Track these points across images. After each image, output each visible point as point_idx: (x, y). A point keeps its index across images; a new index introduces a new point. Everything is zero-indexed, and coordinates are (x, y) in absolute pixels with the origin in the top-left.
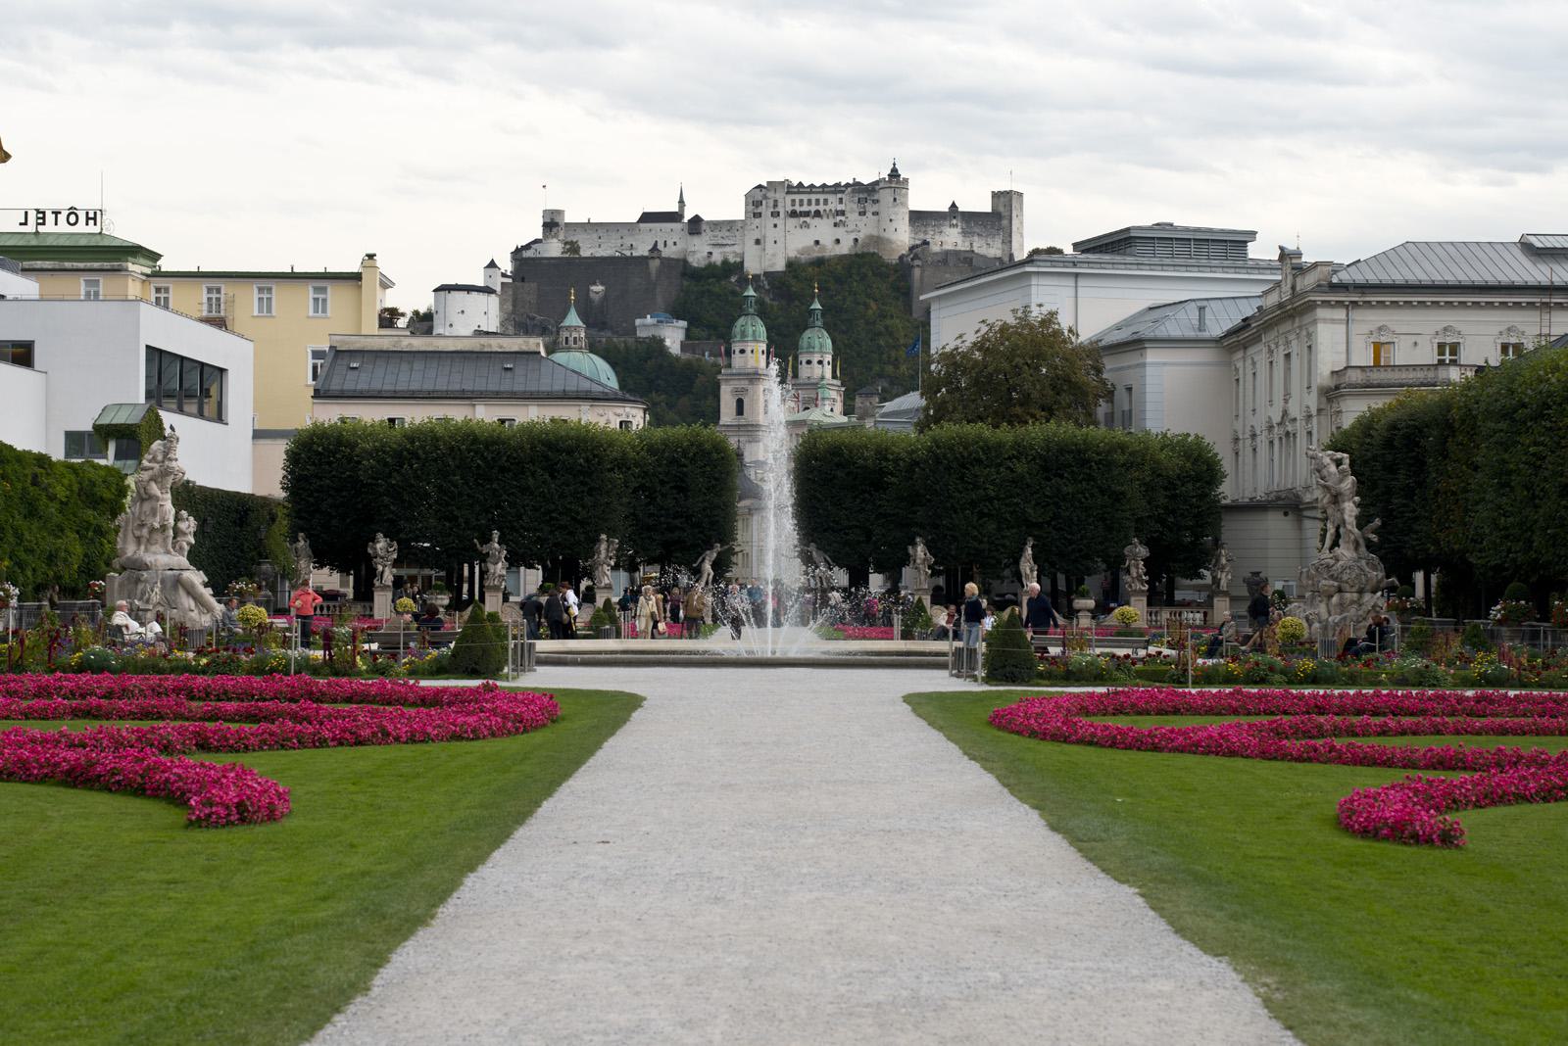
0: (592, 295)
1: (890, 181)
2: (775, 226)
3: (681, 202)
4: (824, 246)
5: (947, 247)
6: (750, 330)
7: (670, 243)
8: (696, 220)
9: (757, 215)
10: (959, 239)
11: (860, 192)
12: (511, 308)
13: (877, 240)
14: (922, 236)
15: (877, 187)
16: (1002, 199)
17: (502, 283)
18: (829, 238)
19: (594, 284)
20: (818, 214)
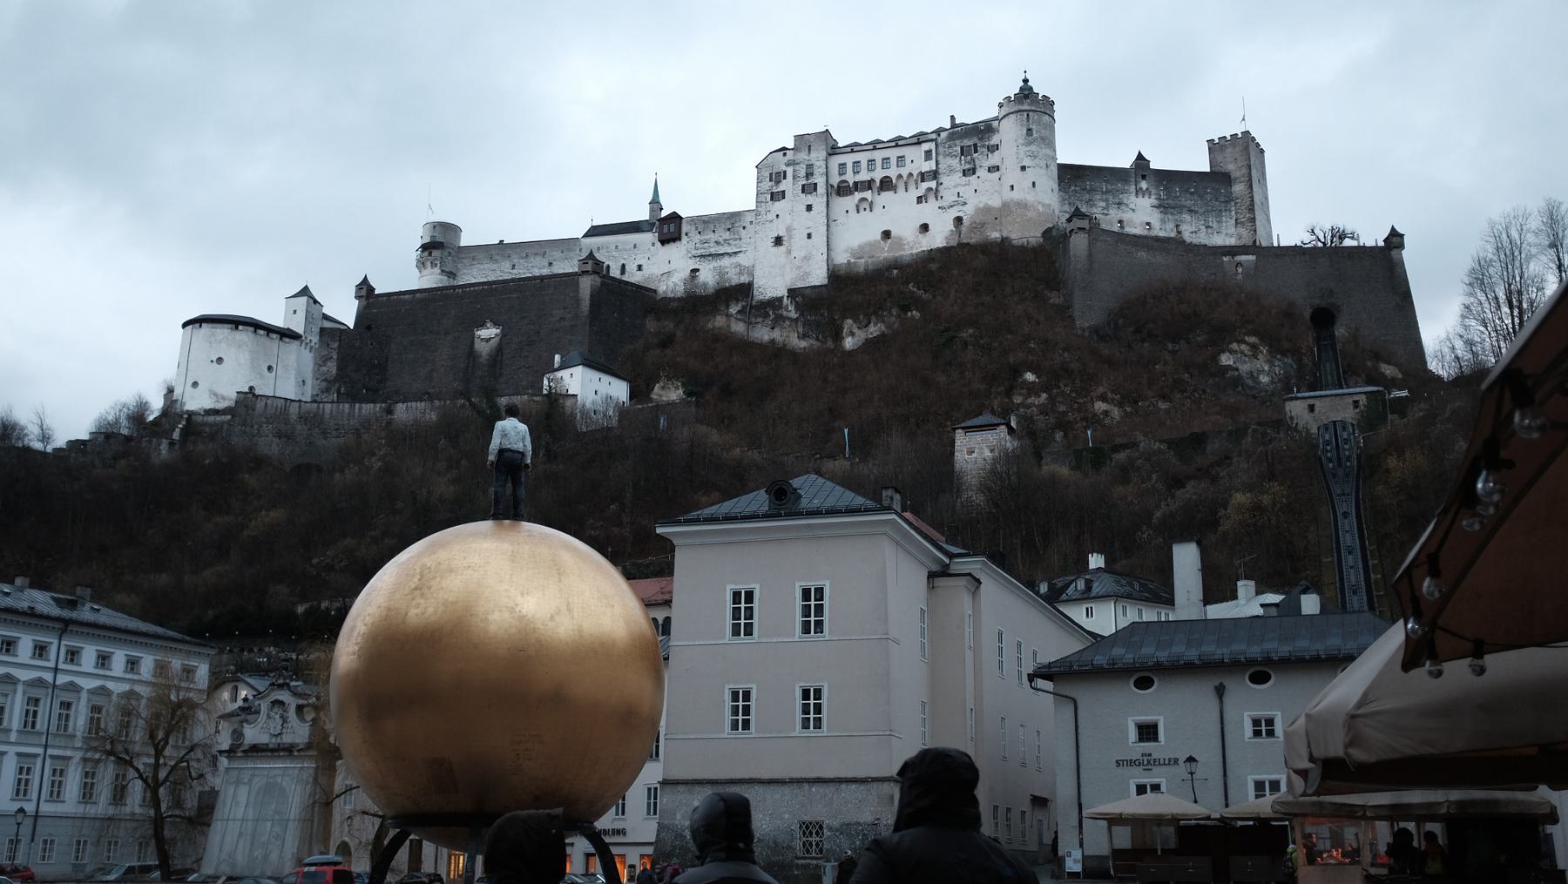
0: (479, 346)
2: (809, 208)
3: (655, 203)
4: (901, 239)
7: (631, 267)
8: (675, 218)
9: (777, 196)
10: (1155, 218)
12: (334, 371)
16: (1229, 150)
17: (322, 330)
19: (482, 325)
20: (886, 185)
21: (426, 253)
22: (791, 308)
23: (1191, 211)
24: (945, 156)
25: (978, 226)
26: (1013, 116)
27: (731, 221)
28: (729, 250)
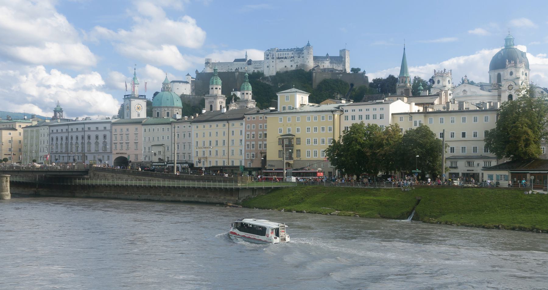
1: (307, 47)
2: (273, 62)
3: (246, 55)
5: (325, 67)
6: (215, 81)
9: (268, 59)
10: (330, 64)
11: (298, 51)
12: (194, 88)
13: (303, 65)
14: (317, 64)
15: (303, 49)
16: (343, 52)
17: (191, 80)
18: (289, 65)
20: (286, 58)
21: (206, 64)
22: (270, 79)
23: (335, 63)
24: (295, 54)
25: (299, 68)
26: (306, 50)
27: (261, 61)
28: (260, 67)
